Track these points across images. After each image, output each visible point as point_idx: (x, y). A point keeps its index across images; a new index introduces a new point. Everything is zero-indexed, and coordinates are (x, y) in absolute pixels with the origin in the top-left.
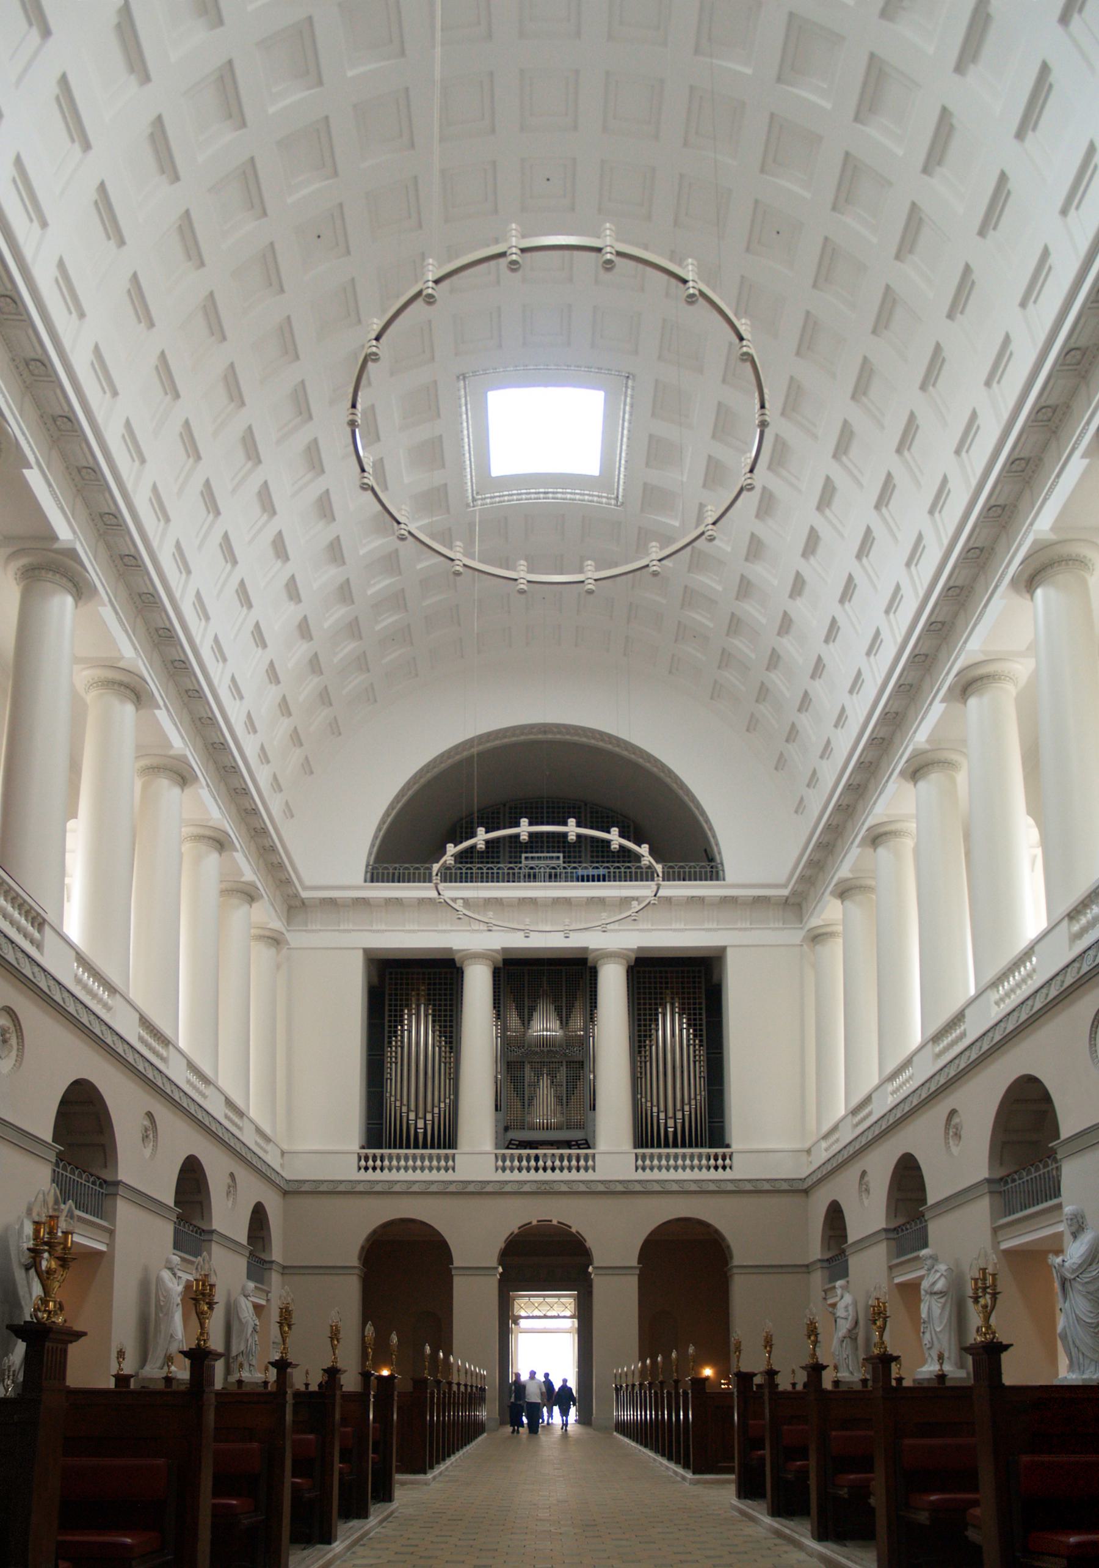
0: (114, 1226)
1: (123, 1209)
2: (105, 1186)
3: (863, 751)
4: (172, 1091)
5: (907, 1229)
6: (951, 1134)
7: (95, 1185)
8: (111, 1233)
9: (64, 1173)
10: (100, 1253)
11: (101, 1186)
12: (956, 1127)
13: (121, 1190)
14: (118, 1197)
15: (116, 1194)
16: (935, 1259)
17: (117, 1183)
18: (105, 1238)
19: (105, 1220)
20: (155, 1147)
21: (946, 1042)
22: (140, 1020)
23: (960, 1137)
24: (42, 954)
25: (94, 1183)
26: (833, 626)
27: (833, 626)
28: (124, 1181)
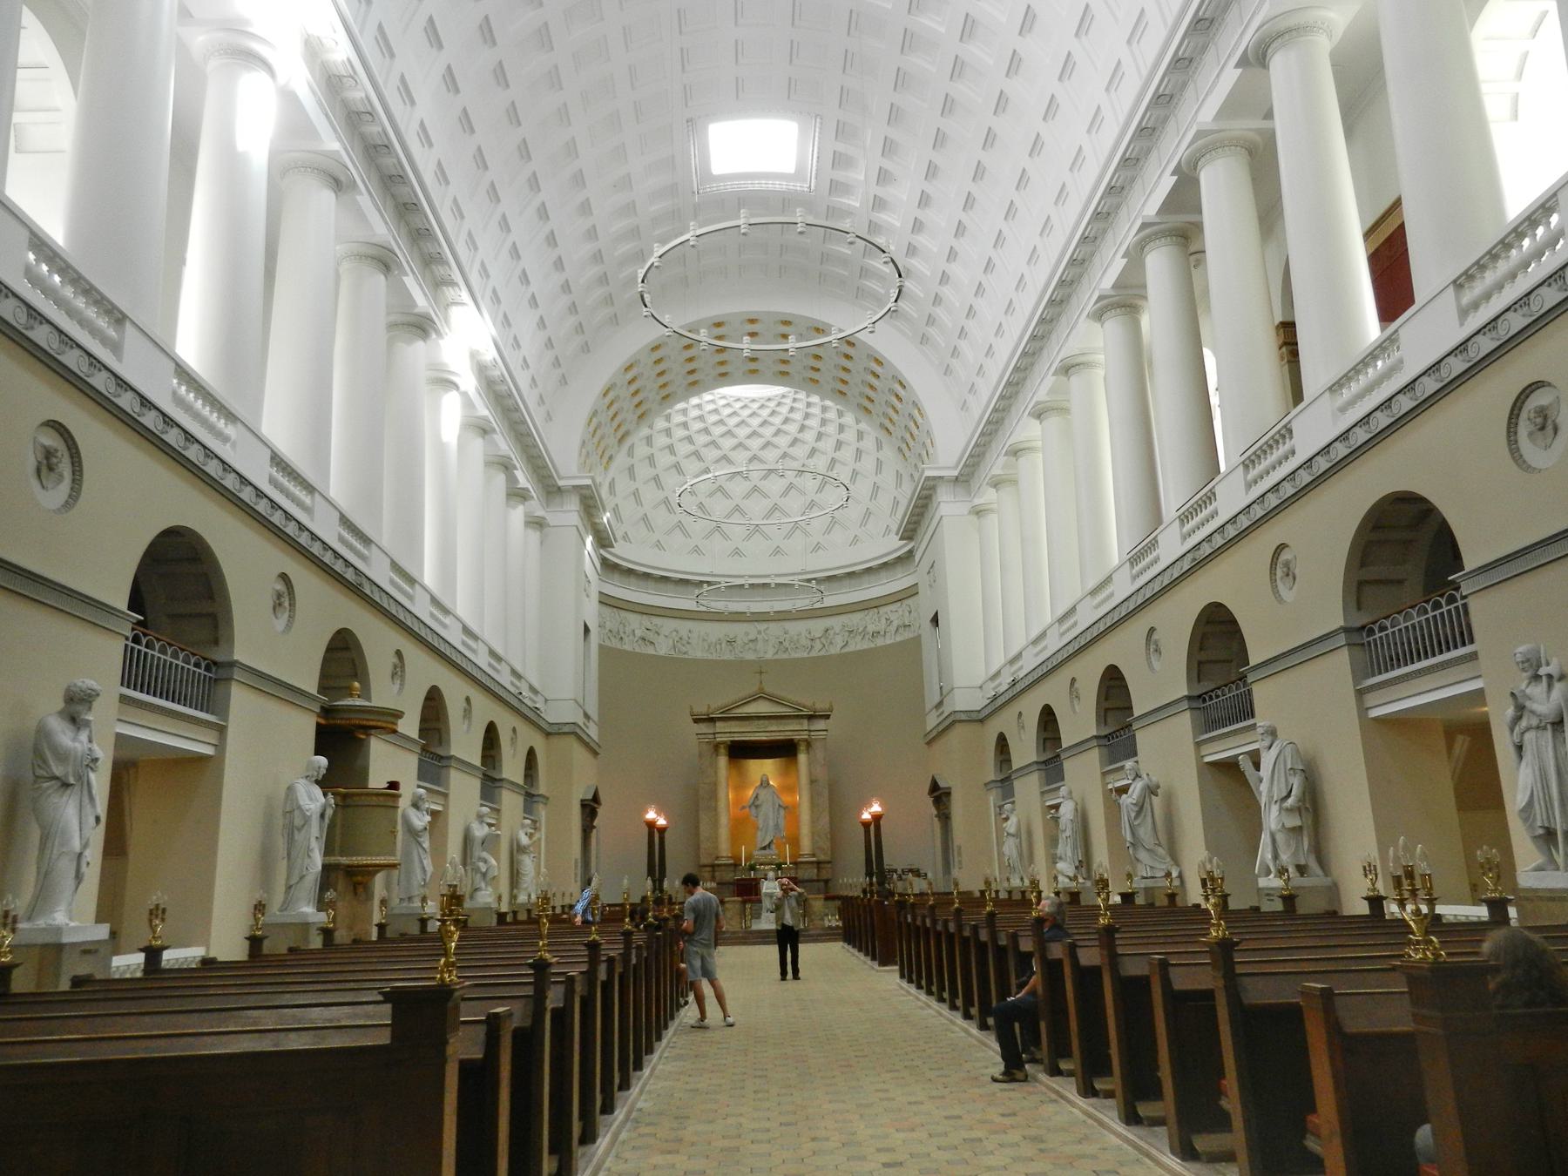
0: (226, 721)
1: (240, 699)
2: (214, 669)
3: (1102, 198)
4: (372, 592)
5: (1217, 697)
6: (1279, 573)
7: (200, 668)
8: (221, 730)
9: (137, 647)
10: (201, 759)
11: (208, 669)
12: (1287, 564)
13: (237, 674)
14: (233, 683)
15: (229, 679)
16: (1272, 733)
17: (233, 664)
18: (212, 737)
19: (212, 714)
20: (291, 617)
21: (1265, 464)
22: (272, 458)
23: (1294, 578)
24: (120, 359)
25: (197, 665)
26: (1068, 62)
27: (1068, 62)
28: (241, 661)
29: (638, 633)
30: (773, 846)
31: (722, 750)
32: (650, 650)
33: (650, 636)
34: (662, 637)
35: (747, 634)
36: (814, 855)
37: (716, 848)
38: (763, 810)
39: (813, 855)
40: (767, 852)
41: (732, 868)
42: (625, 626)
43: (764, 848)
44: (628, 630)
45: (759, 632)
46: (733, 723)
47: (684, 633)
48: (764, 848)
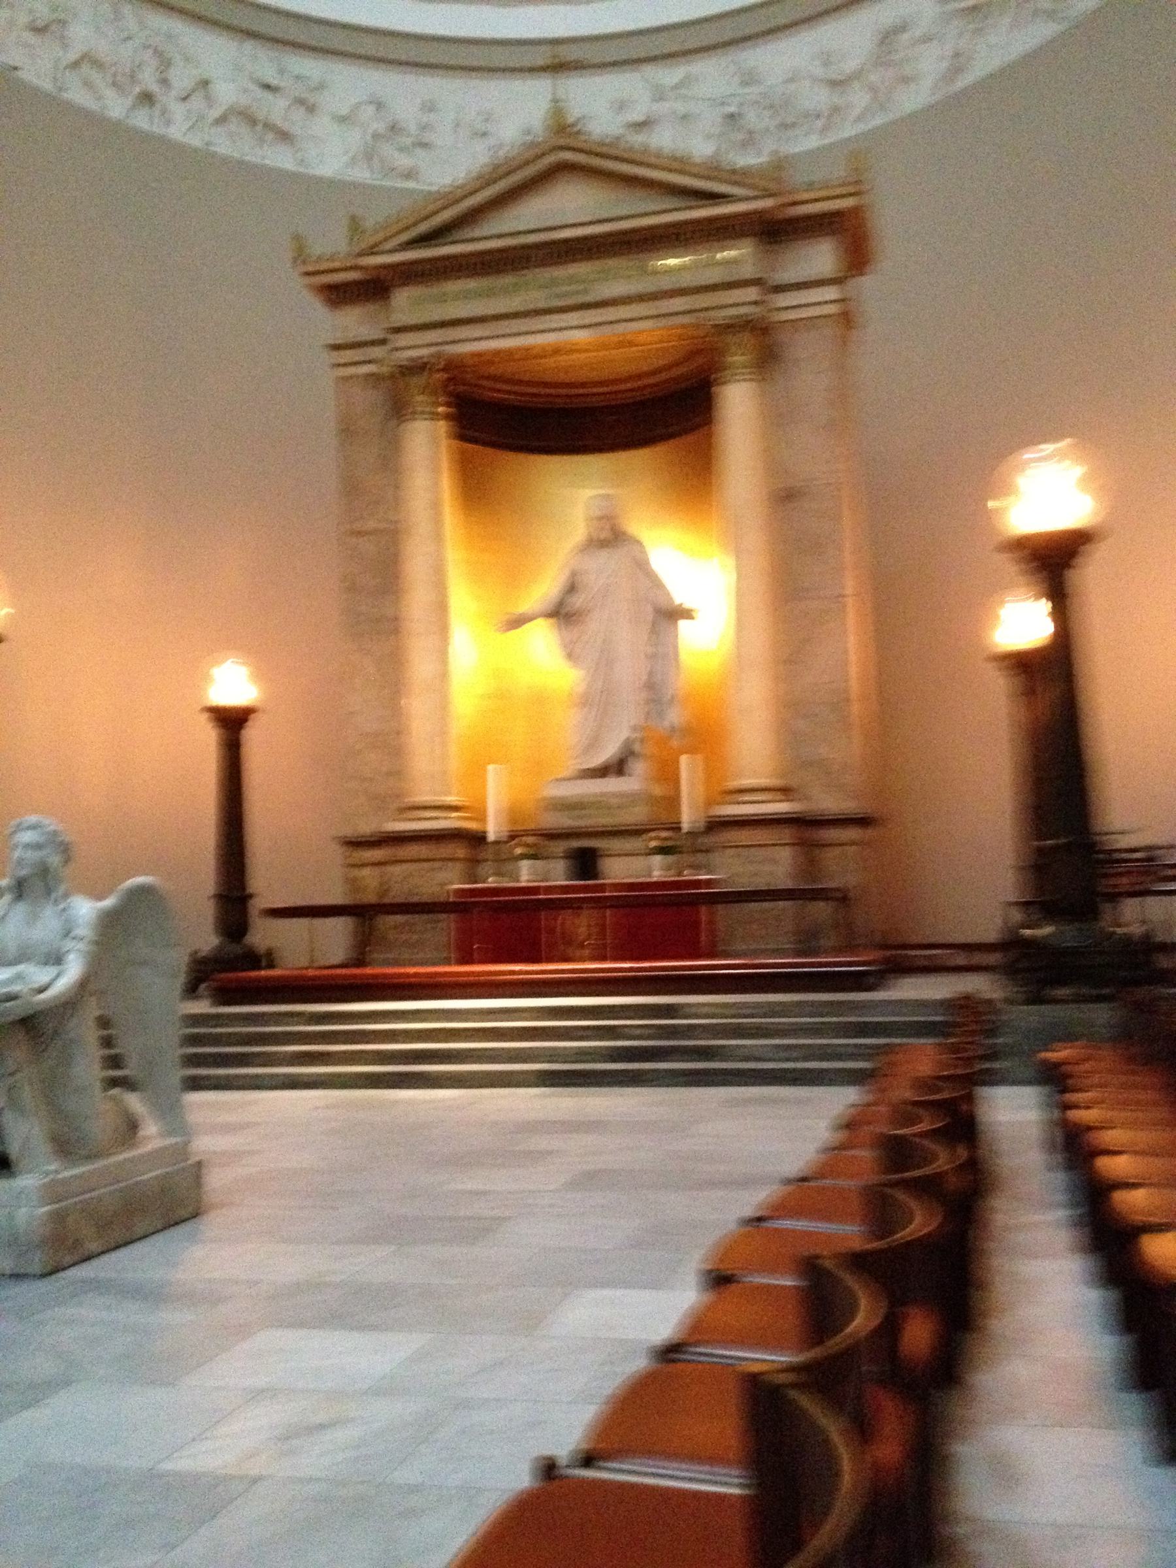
29: (227, 93)
30: (639, 768)
31: (420, 400)
32: (280, 158)
33: (276, 108)
34: (322, 125)
35: (621, 106)
36: (785, 792)
37: (397, 773)
38: (594, 625)
39: (785, 792)
40: (612, 785)
41: (461, 851)
42: (165, 63)
43: (603, 772)
44: (182, 78)
45: (659, 95)
46: (453, 286)
47: (407, 111)
48: (603, 772)
